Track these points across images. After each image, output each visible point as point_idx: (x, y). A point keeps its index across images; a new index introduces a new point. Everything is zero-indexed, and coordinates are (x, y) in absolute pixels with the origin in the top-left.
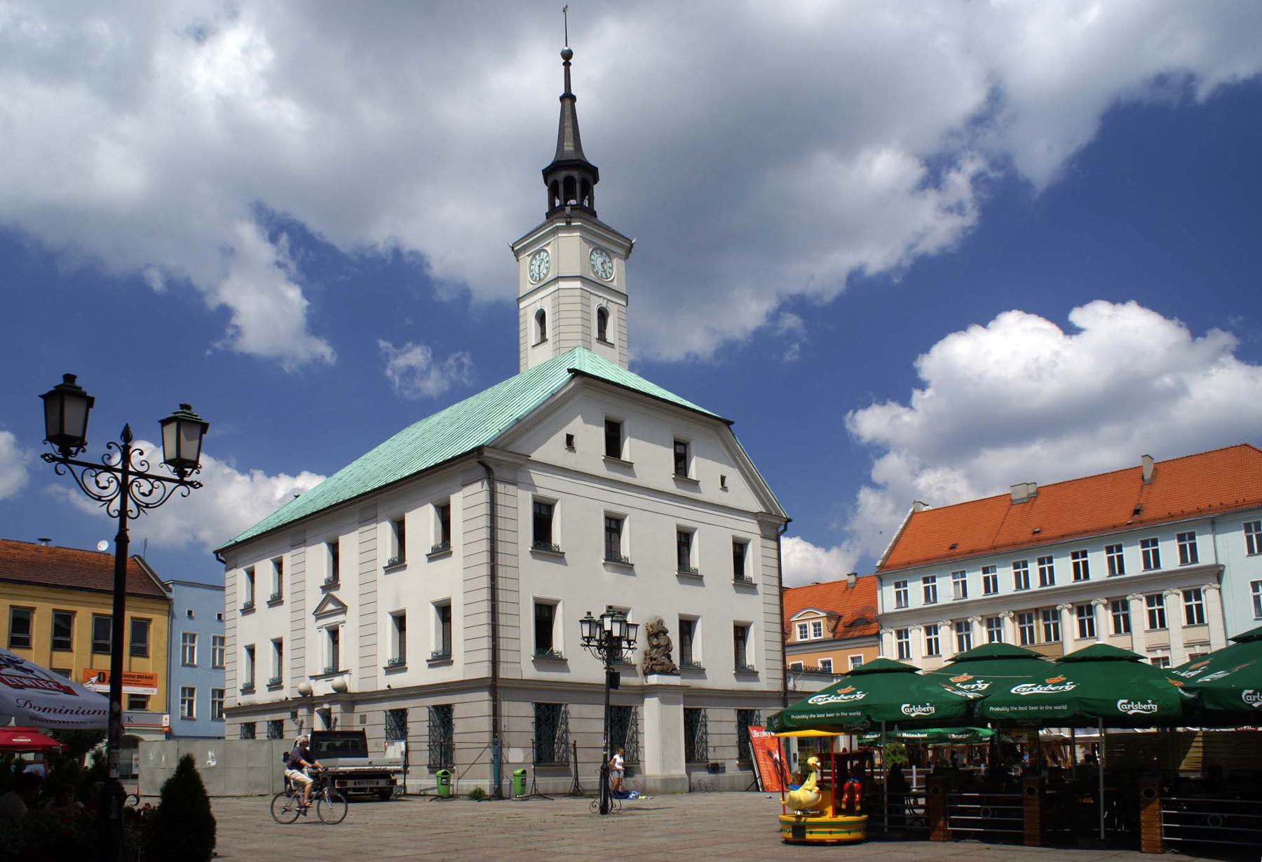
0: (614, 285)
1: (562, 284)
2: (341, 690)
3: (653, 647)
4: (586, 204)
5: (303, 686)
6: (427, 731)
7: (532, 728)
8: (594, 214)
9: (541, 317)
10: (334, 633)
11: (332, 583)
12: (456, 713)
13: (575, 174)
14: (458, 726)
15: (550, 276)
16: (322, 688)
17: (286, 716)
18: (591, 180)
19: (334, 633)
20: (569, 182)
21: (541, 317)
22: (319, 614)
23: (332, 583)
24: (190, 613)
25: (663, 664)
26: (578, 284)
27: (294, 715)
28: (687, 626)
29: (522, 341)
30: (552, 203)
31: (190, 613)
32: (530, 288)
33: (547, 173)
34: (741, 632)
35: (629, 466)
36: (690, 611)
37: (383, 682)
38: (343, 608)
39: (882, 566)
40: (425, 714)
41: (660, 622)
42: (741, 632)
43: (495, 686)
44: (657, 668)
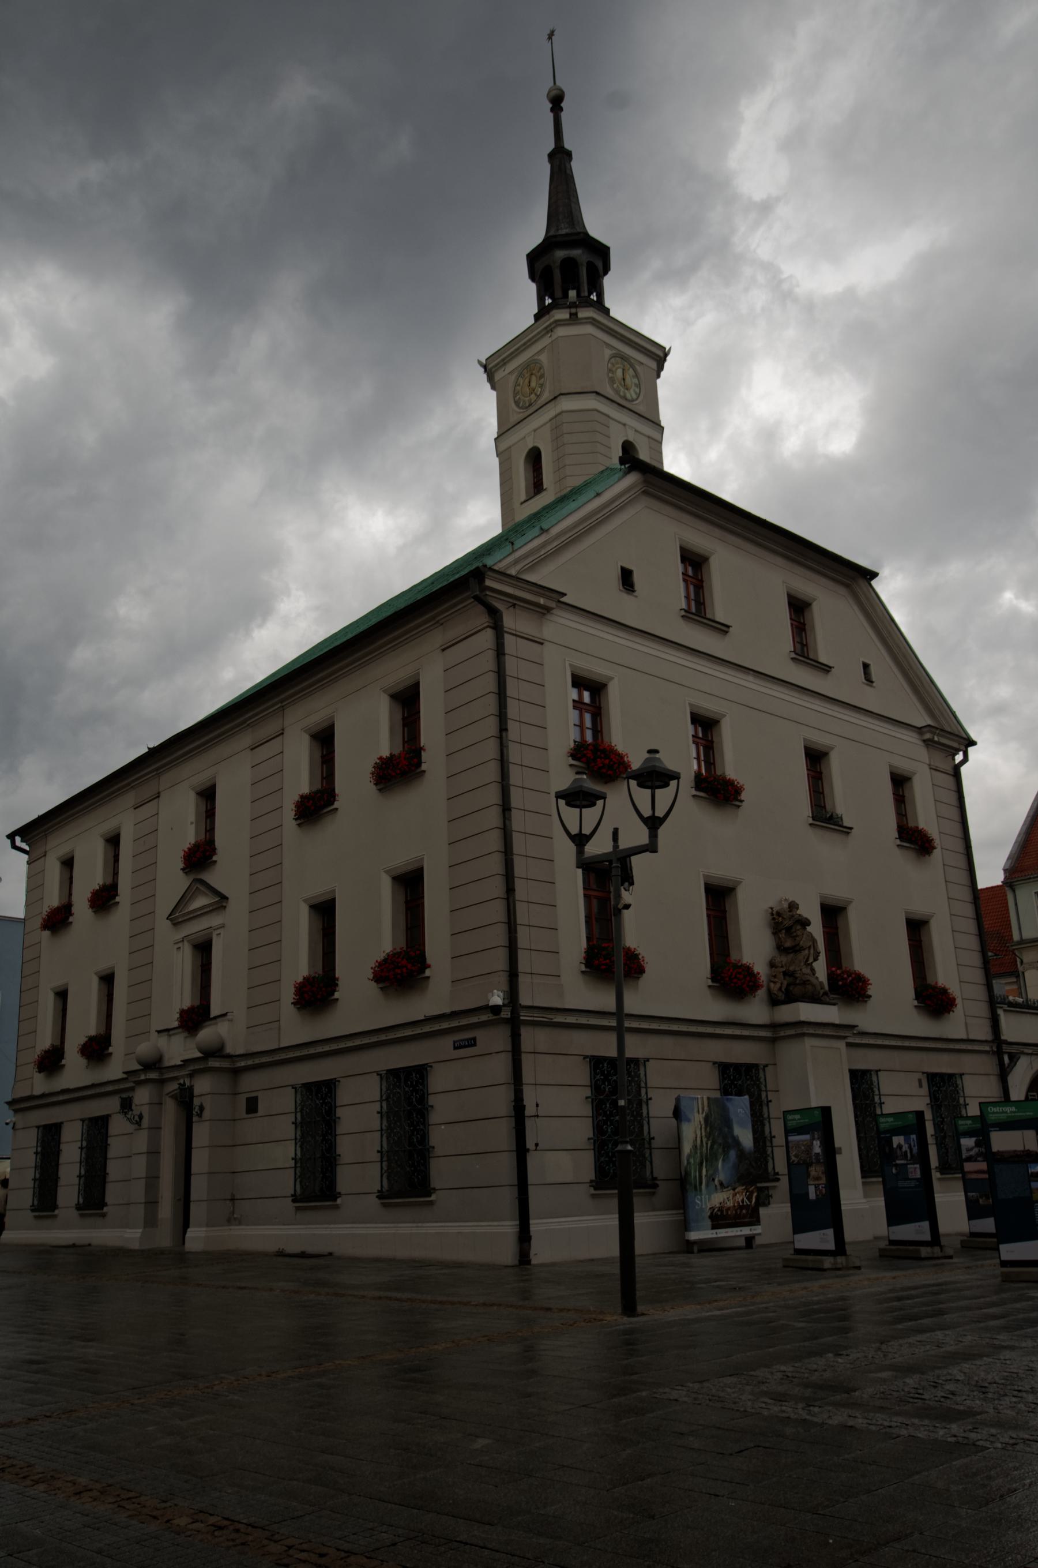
1: (567, 404)
2: (215, 1051)
4: (594, 297)
6: (375, 1122)
7: (587, 1110)
8: (607, 311)
11: (200, 857)
13: (576, 253)
14: (442, 1109)
15: (546, 396)
16: (178, 1050)
17: (110, 1105)
18: (600, 265)
19: (203, 949)
20: (569, 264)
22: (176, 918)
23: (200, 857)
26: (591, 403)
27: (126, 1105)
30: (541, 299)
33: (533, 258)
35: (723, 629)
37: (295, 1029)
38: (222, 900)
40: (372, 1089)
41: (793, 906)
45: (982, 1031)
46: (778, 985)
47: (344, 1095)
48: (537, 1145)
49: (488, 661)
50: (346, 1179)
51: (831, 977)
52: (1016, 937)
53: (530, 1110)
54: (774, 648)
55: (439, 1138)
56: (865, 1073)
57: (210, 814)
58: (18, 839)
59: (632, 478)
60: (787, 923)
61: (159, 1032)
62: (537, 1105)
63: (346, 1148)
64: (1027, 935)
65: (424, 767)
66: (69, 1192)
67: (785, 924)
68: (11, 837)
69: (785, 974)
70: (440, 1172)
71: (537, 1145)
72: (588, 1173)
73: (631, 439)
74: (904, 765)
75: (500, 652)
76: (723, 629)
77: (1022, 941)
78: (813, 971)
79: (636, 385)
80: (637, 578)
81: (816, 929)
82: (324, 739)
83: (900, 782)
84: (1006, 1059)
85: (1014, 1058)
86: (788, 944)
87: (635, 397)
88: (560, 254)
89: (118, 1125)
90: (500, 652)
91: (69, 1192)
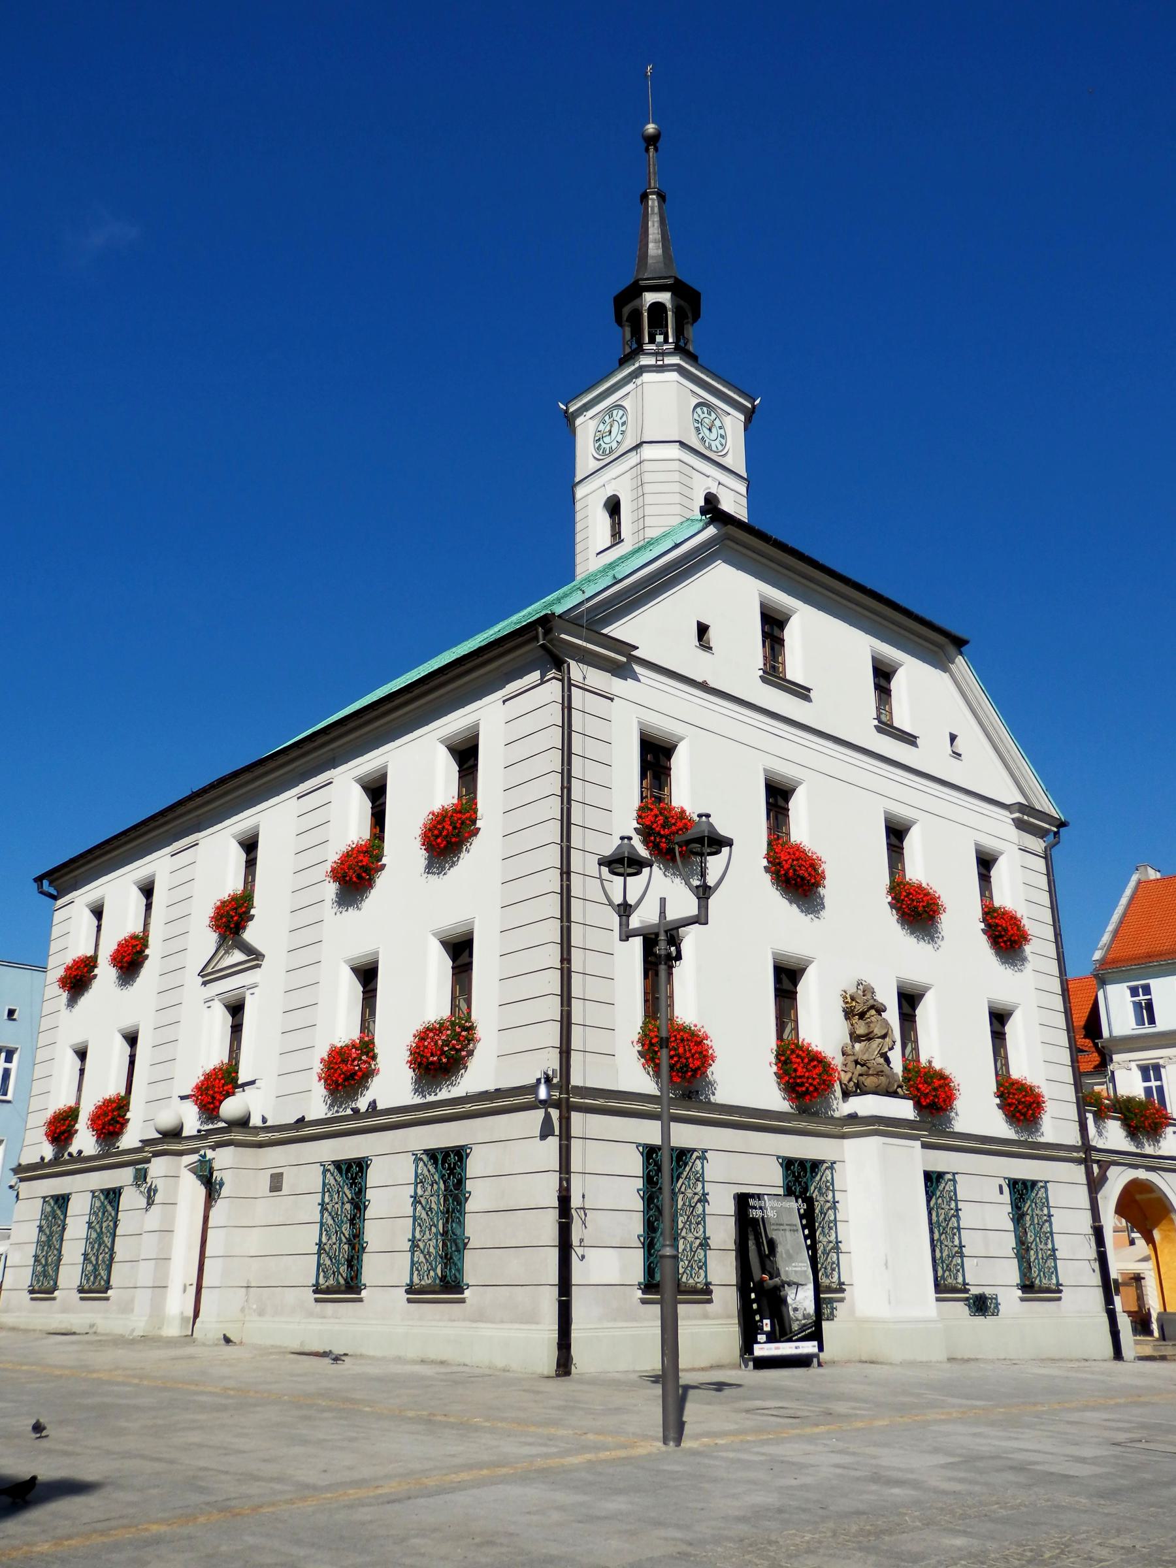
0: (728, 461)
3: (855, 1038)
5: (167, 1120)
9: (613, 507)
10: (236, 1009)
12: (474, 1166)
14: (480, 1195)
15: (629, 443)
17: (123, 1177)
19: (236, 1009)
21: (613, 507)
22: (208, 976)
24: (11, 1013)
25: (879, 1073)
26: (674, 451)
27: (141, 1177)
28: (909, 1000)
29: (578, 548)
31: (11, 1013)
32: (593, 465)
34: (999, 1018)
35: (802, 692)
36: (915, 976)
38: (255, 956)
39: (1103, 962)
40: (405, 1170)
41: (868, 990)
42: (999, 1018)
43: (562, 1101)
44: (870, 1082)
45: (1072, 1137)
46: (849, 1075)
47: (374, 1176)
48: (582, 1240)
49: (555, 714)
50: (372, 1269)
51: (906, 1069)
52: (1106, 1033)
53: (575, 1202)
54: (854, 712)
55: (474, 1228)
56: (940, 1175)
57: (251, 864)
58: (45, 883)
59: (711, 531)
60: (859, 1008)
61: (182, 1098)
62: (583, 1196)
63: (373, 1233)
64: (1117, 1032)
65: (479, 824)
66: (70, 1274)
67: (859, 1009)
68: (39, 880)
69: (856, 1062)
70: (474, 1267)
71: (582, 1240)
72: (638, 1275)
73: (714, 491)
74: (990, 843)
75: (567, 707)
76: (802, 692)
77: (1112, 1039)
78: (887, 1061)
79: (722, 436)
80: (712, 634)
81: (892, 1015)
82: (376, 790)
83: (985, 863)
84: (1095, 1168)
85: (1104, 1166)
86: (861, 1030)
87: (720, 448)
88: (650, 298)
89: (131, 1199)
90: (567, 707)
91: (70, 1274)
